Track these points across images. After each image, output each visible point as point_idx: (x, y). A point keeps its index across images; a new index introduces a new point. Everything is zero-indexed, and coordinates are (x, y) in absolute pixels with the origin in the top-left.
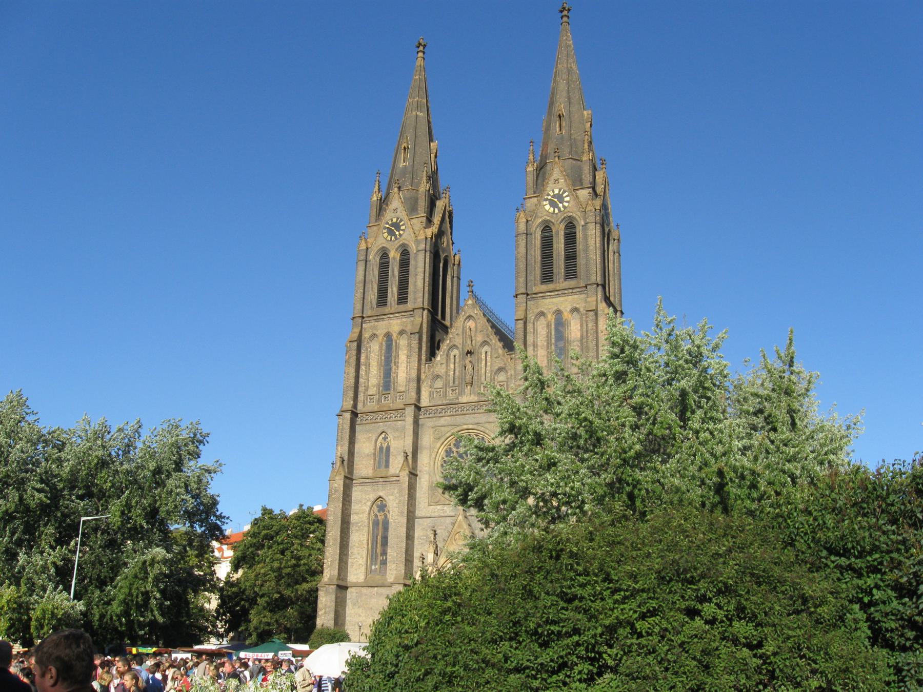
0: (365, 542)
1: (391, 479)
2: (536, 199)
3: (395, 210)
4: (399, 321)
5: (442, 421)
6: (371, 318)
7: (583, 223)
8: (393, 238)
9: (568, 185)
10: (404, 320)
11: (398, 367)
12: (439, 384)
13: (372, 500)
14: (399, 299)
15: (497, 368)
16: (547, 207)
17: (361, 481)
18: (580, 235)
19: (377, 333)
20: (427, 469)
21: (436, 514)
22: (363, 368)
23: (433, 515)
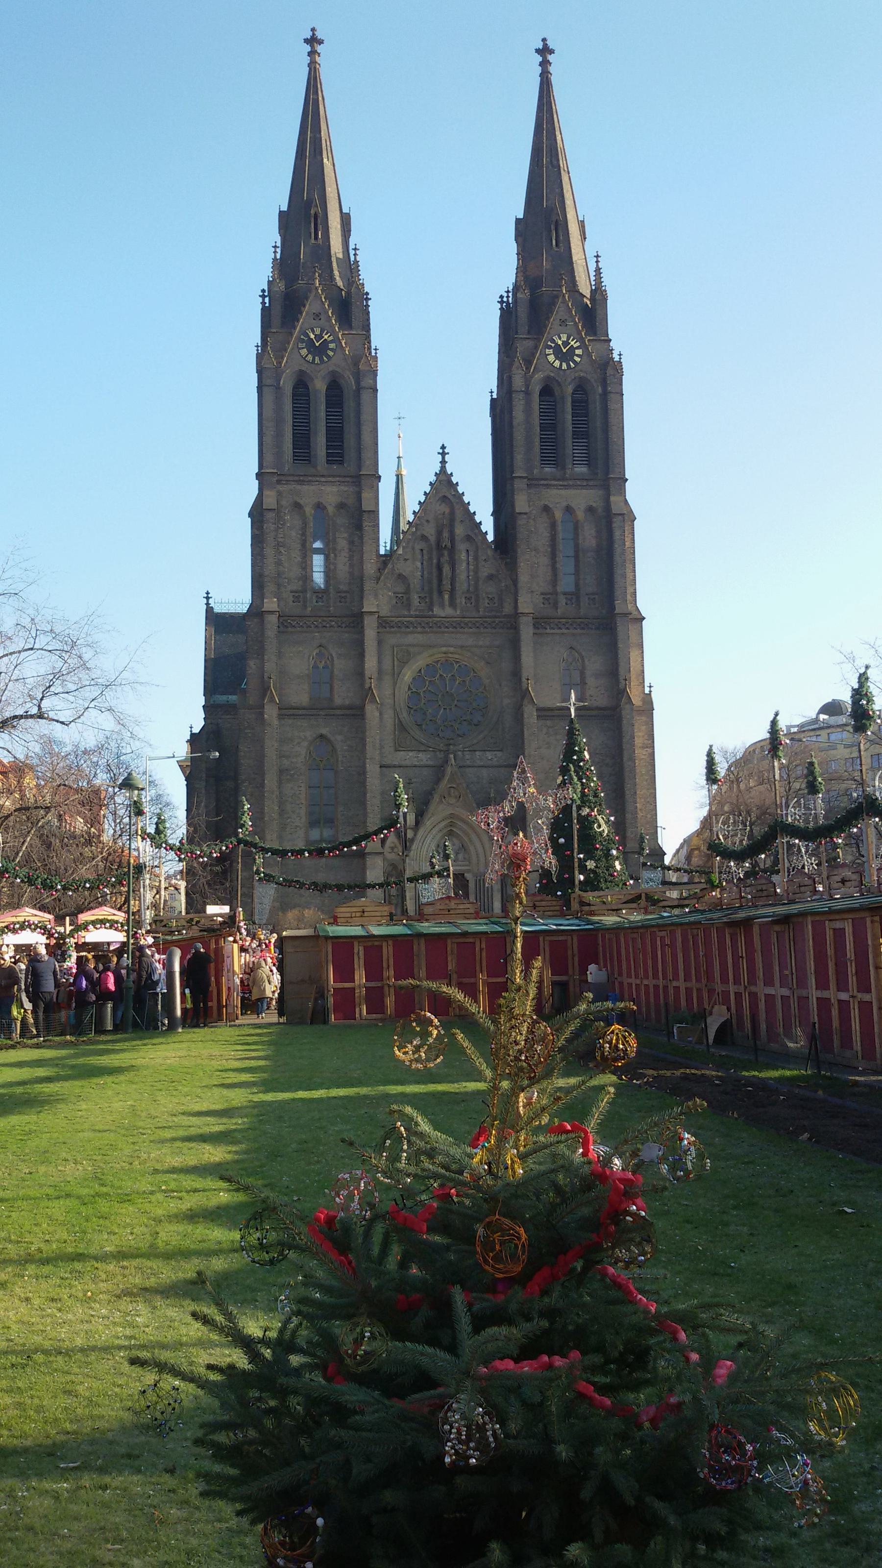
0: (303, 796)
1: (338, 712)
2: (530, 344)
3: (317, 316)
4: (335, 489)
5: (410, 639)
6: (291, 478)
7: (600, 390)
8: (317, 360)
9: (579, 333)
10: (342, 487)
11: (336, 556)
12: (400, 588)
13: (310, 738)
14: (328, 455)
15: (486, 574)
16: (551, 358)
17: (292, 712)
18: (596, 407)
19: (302, 502)
20: (390, 701)
21: (408, 763)
22: (282, 550)
23: (404, 763)
